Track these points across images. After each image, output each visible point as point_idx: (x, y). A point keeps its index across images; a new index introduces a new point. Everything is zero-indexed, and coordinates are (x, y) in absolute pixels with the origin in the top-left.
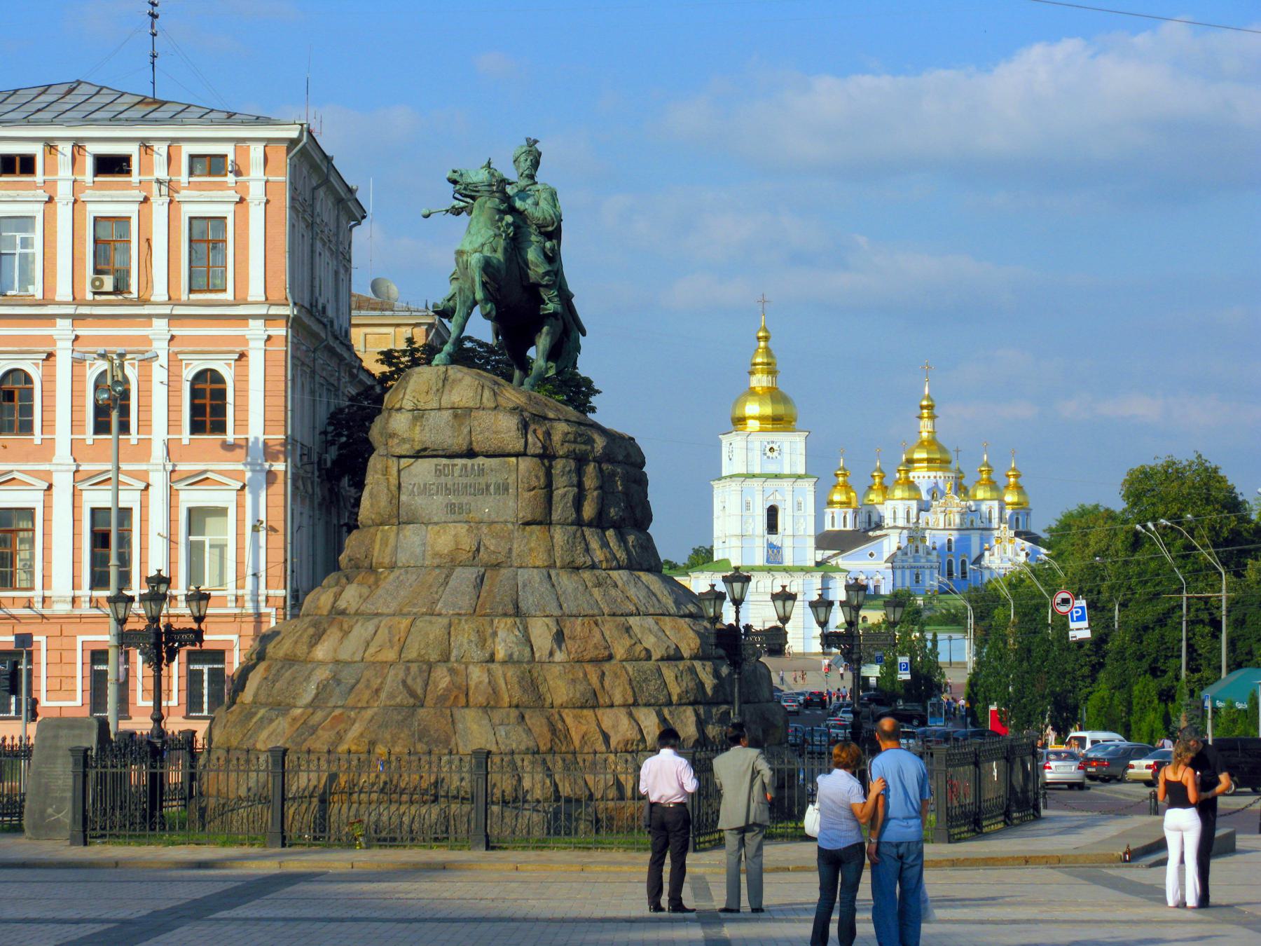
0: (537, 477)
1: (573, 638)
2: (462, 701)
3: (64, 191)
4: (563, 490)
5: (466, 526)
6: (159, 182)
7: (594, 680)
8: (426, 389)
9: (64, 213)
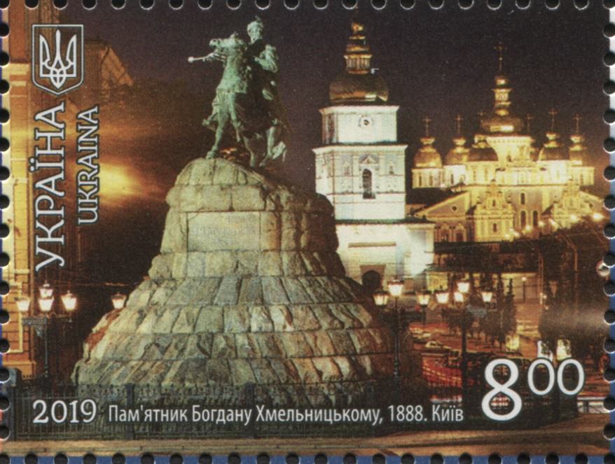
0: (272, 224)
1: (297, 318)
2: (234, 355)
4: (288, 231)
7: (310, 341)
8: (203, 172)
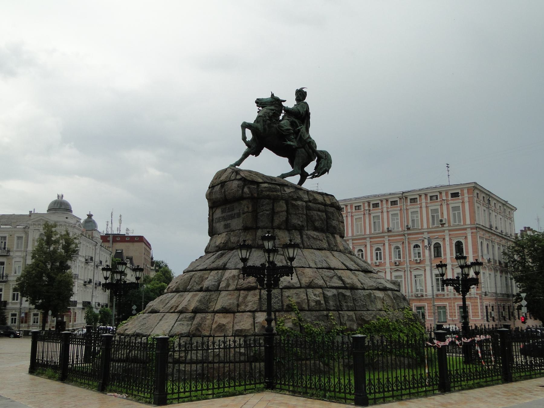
0: (248, 207)
3: (424, 205)
5: (226, 233)
6: (444, 200)
9: (424, 210)
